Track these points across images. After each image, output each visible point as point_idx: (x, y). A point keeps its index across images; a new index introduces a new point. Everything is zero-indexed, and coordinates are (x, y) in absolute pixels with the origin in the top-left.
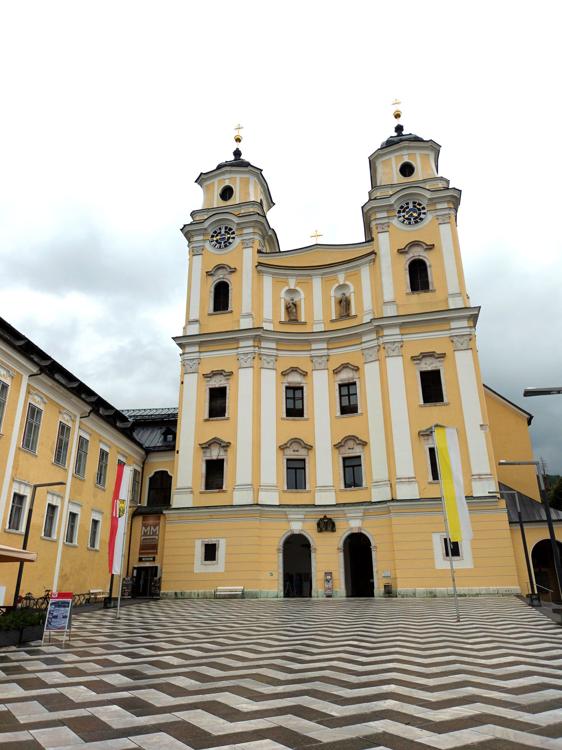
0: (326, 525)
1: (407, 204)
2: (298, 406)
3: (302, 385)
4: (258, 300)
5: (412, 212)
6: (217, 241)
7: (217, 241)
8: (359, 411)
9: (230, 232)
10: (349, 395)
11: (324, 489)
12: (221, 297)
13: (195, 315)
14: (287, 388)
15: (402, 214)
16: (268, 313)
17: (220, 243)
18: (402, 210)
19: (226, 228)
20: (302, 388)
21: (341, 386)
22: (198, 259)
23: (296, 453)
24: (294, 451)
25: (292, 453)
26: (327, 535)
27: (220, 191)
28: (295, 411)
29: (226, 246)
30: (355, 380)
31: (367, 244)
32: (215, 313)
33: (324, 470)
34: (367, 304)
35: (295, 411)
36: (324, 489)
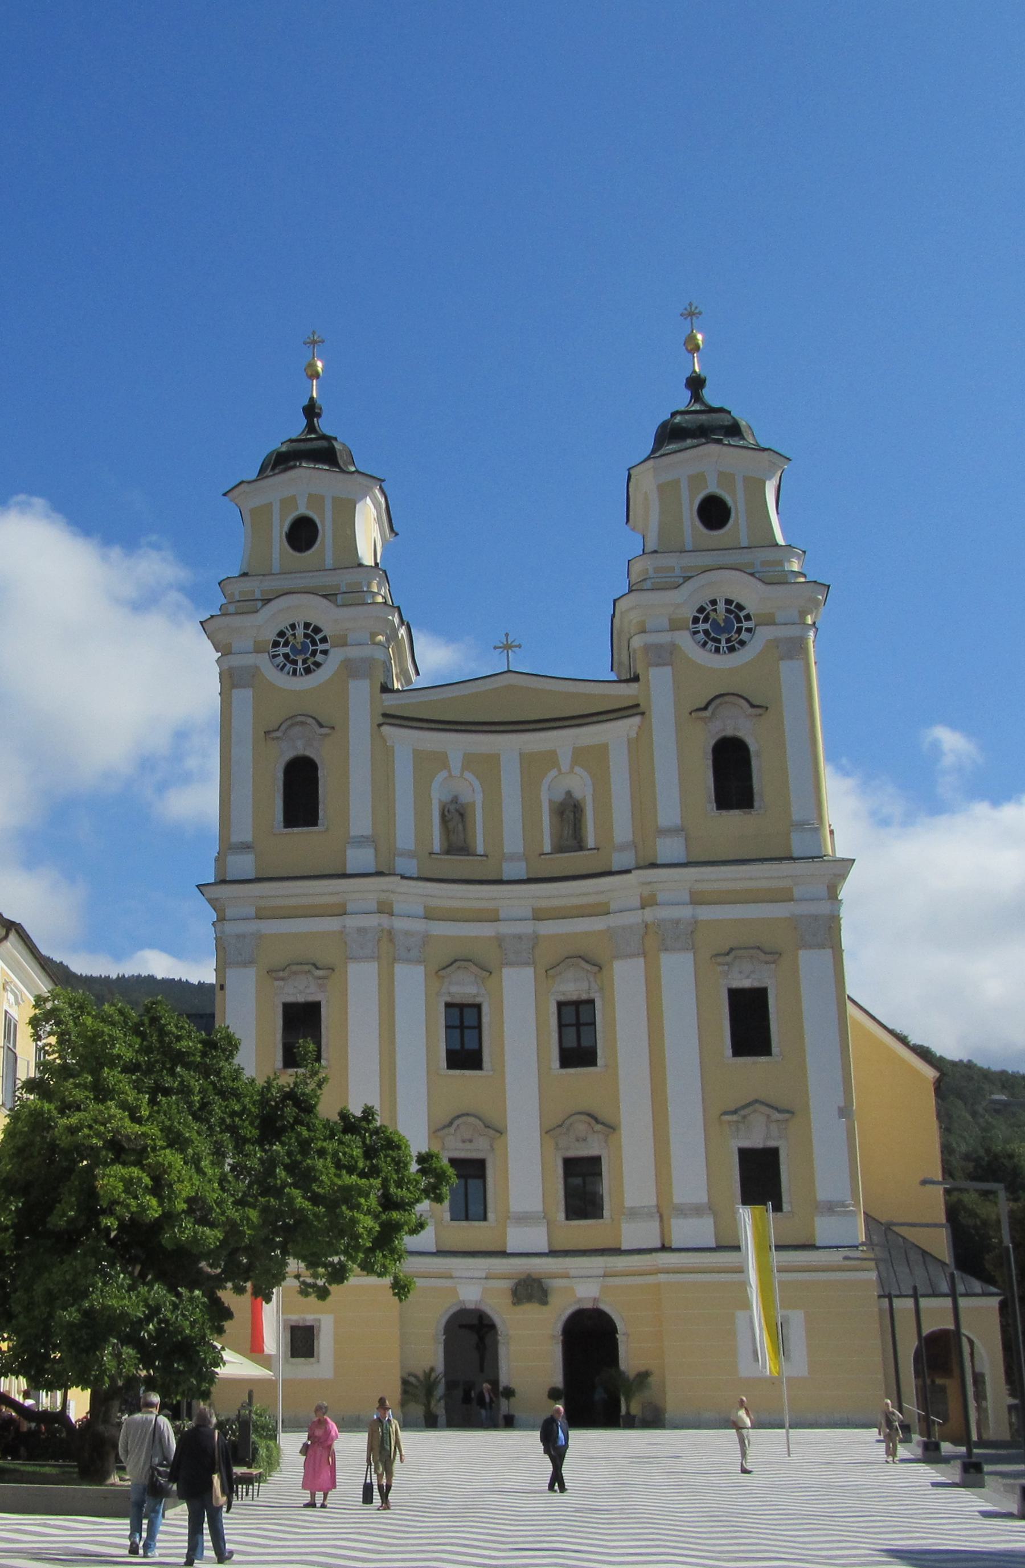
0: (530, 1290)
1: (714, 602)
2: (470, 1045)
3: (478, 1000)
4: (376, 790)
5: (723, 626)
6: (286, 656)
7: (286, 656)
8: (600, 1061)
9: (317, 637)
10: (578, 1025)
11: (524, 1219)
12: (301, 793)
13: (243, 833)
14: (448, 1005)
15: (702, 626)
16: (405, 836)
17: (295, 662)
18: (702, 616)
19: (307, 625)
20: (478, 1007)
21: (560, 1005)
22: (243, 696)
23: (468, 1146)
24: (464, 1141)
25: (461, 1145)
26: (531, 1311)
27: (286, 528)
28: (465, 1056)
29: (308, 671)
30: (592, 995)
31: (623, 685)
32: (290, 830)
33: (525, 1181)
34: (622, 830)
35: (465, 1056)
36: (524, 1219)
